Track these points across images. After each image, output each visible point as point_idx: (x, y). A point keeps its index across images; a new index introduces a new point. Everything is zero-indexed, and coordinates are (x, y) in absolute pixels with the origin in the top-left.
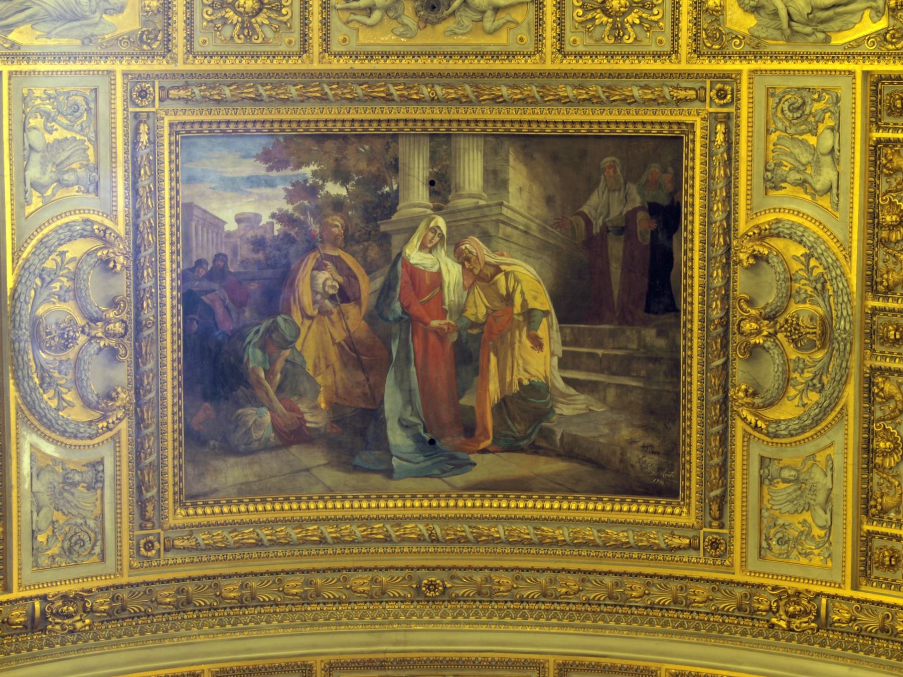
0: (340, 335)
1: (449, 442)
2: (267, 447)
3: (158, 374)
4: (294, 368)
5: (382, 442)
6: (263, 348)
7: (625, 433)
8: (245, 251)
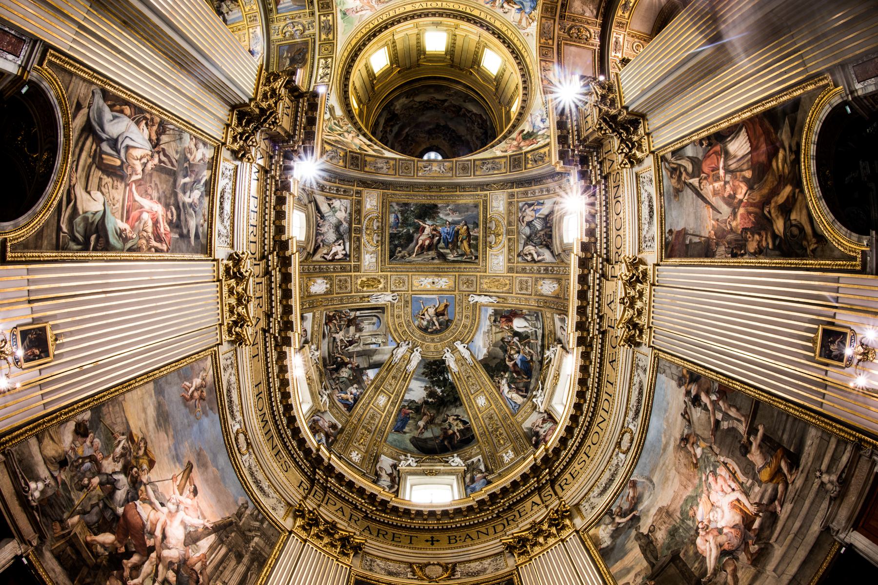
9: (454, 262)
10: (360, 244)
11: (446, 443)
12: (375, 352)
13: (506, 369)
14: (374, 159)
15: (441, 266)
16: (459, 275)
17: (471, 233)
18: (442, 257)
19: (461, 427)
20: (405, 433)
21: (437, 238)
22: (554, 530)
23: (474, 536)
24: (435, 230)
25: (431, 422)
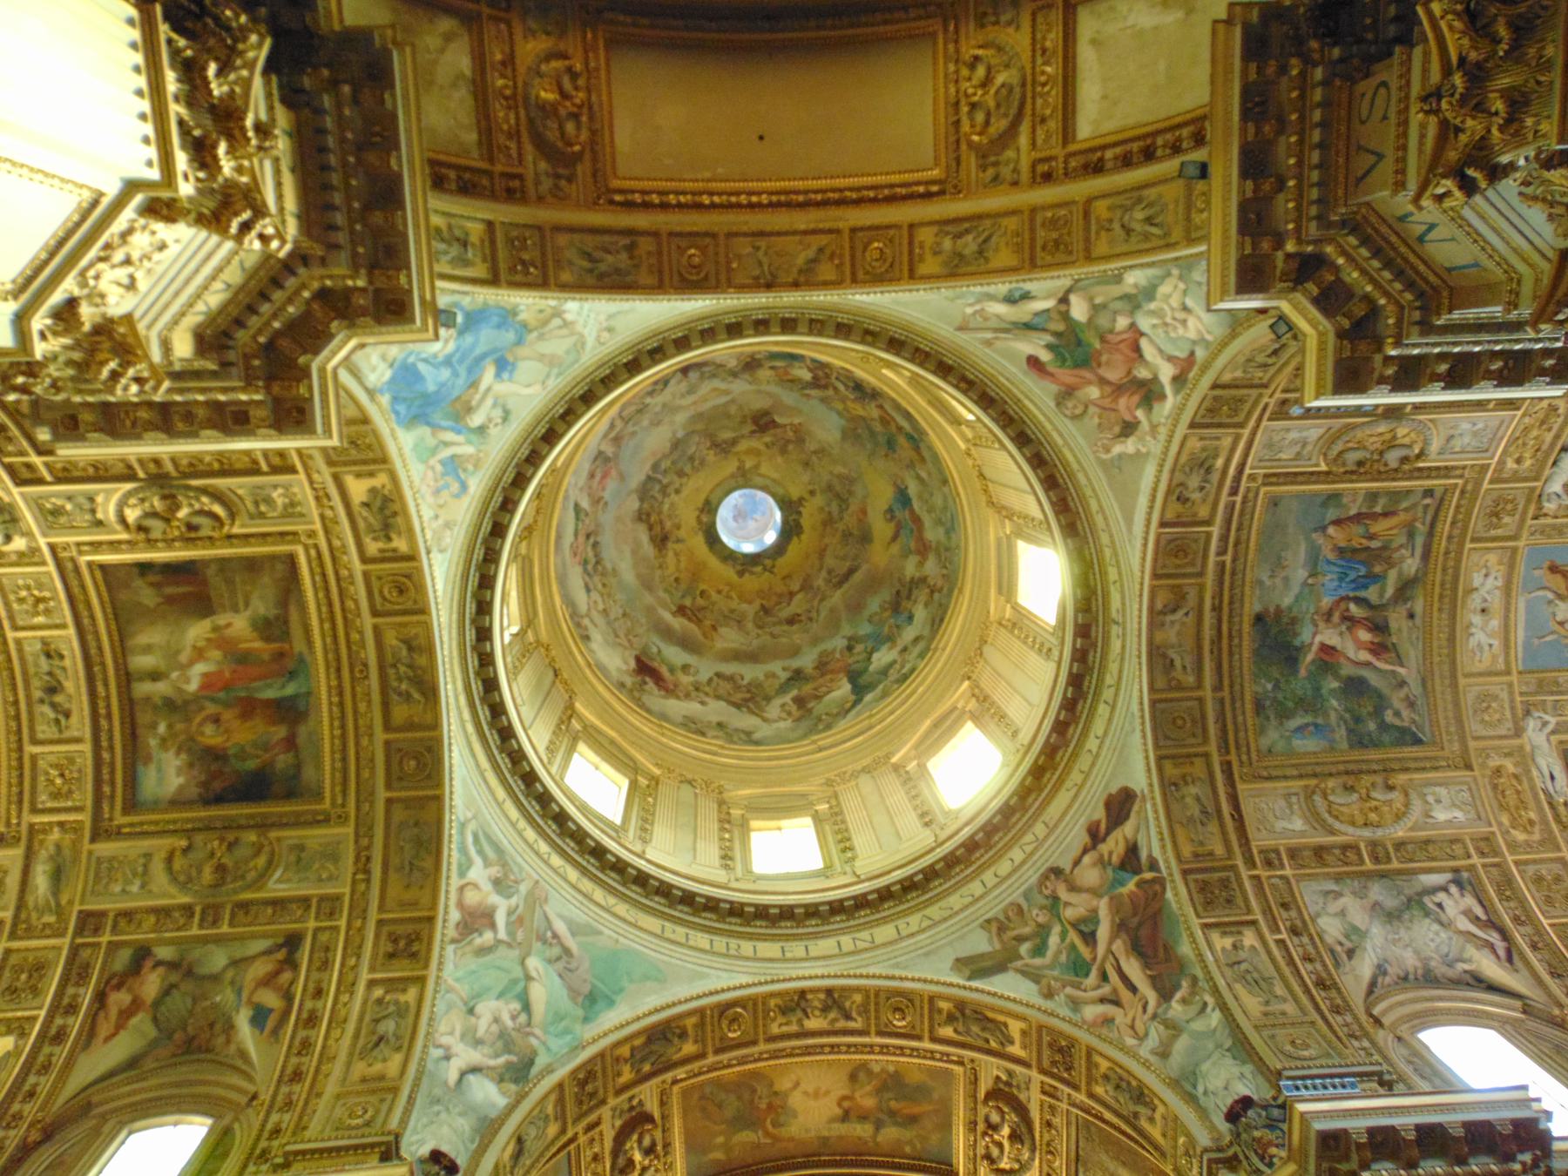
0: (238, 722)
1: (290, 664)
2: (297, 756)
3: (252, 816)
4: (255, 744)
5: (292, 699)
6: (244, 760)
7: (266, 579)
8: (195, 772)
9: (1426, 556)
10: (1412, 841)
14: (1178, 828)
15: (1437, 590)
16: (1474, 540)
17: (1353, 512)
18: (1405, 589)
21: (1353, 607)
24: (1328, 616)
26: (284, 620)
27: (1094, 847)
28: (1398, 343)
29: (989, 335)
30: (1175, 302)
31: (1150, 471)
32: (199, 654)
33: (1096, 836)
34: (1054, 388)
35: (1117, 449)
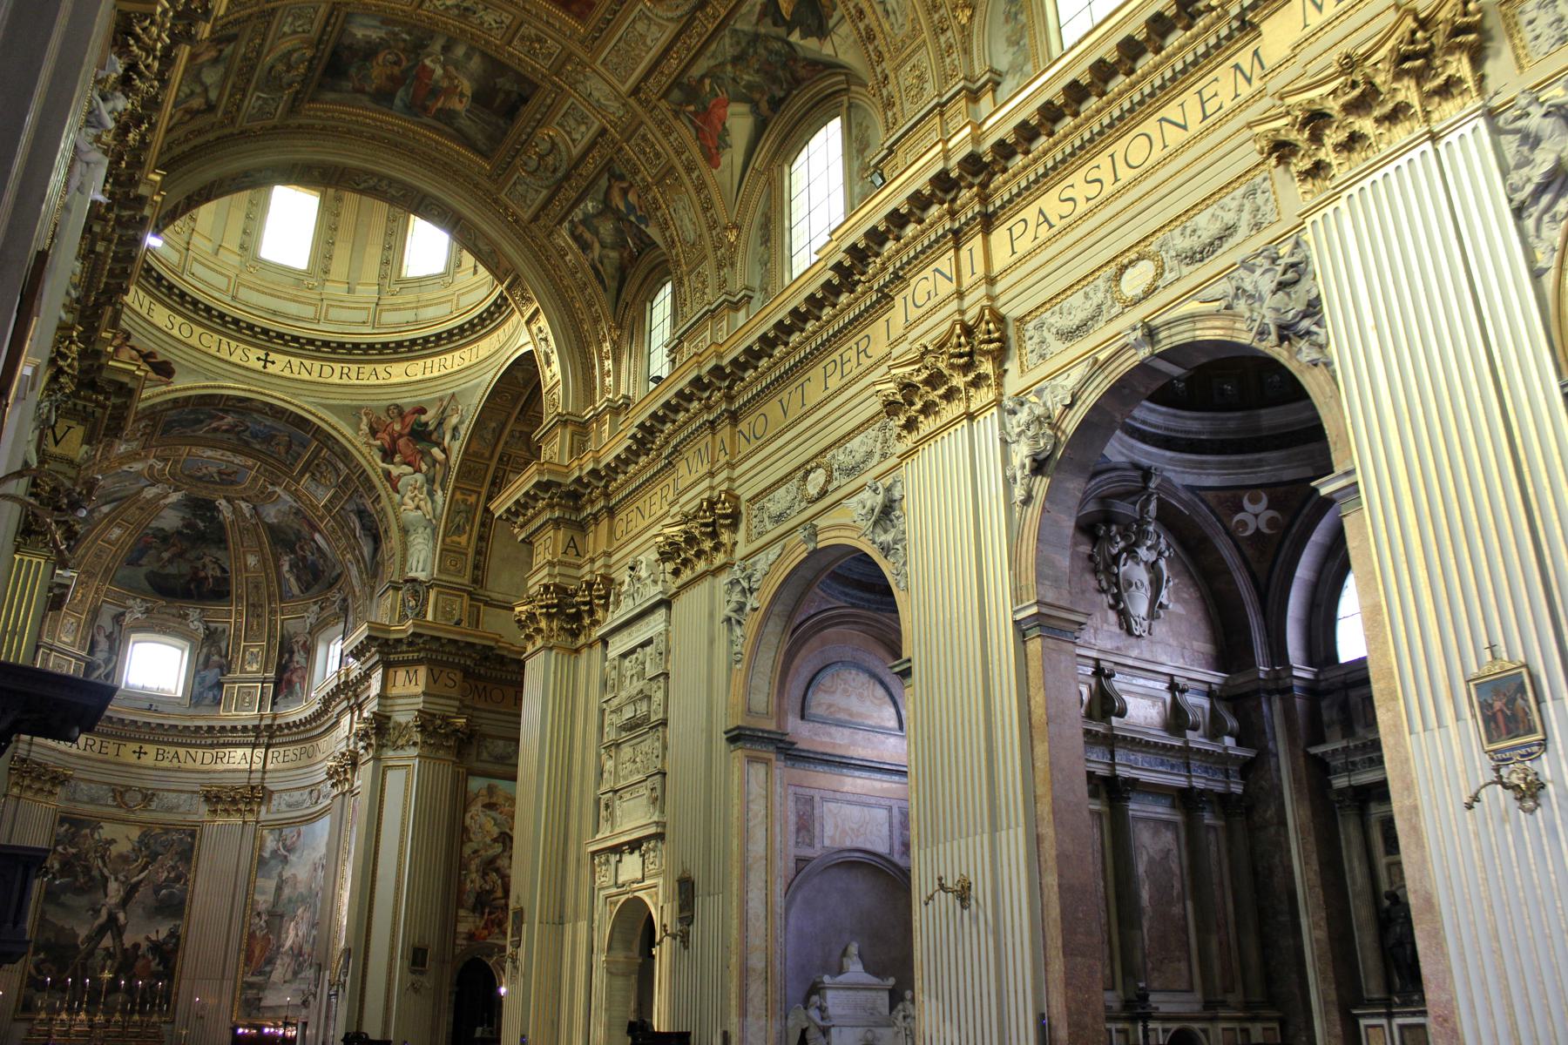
5: (392, 101)
7: (480, 137)
11: (192, 586)
12: (115, 492)
13: (293, 551)
19: (219, 574)
20: (141, 566)
22: (242, 806)
23: (182, 759)
25: (181, 555)
26: (450, 125)
27: (141, 356)
28: (377, 651)
29: (445, 403)
30: (422, 503)
31: (348, 431)
32: (447, 74)
33: (147, 357)
34: (407, 410)
35: (365, 420)
